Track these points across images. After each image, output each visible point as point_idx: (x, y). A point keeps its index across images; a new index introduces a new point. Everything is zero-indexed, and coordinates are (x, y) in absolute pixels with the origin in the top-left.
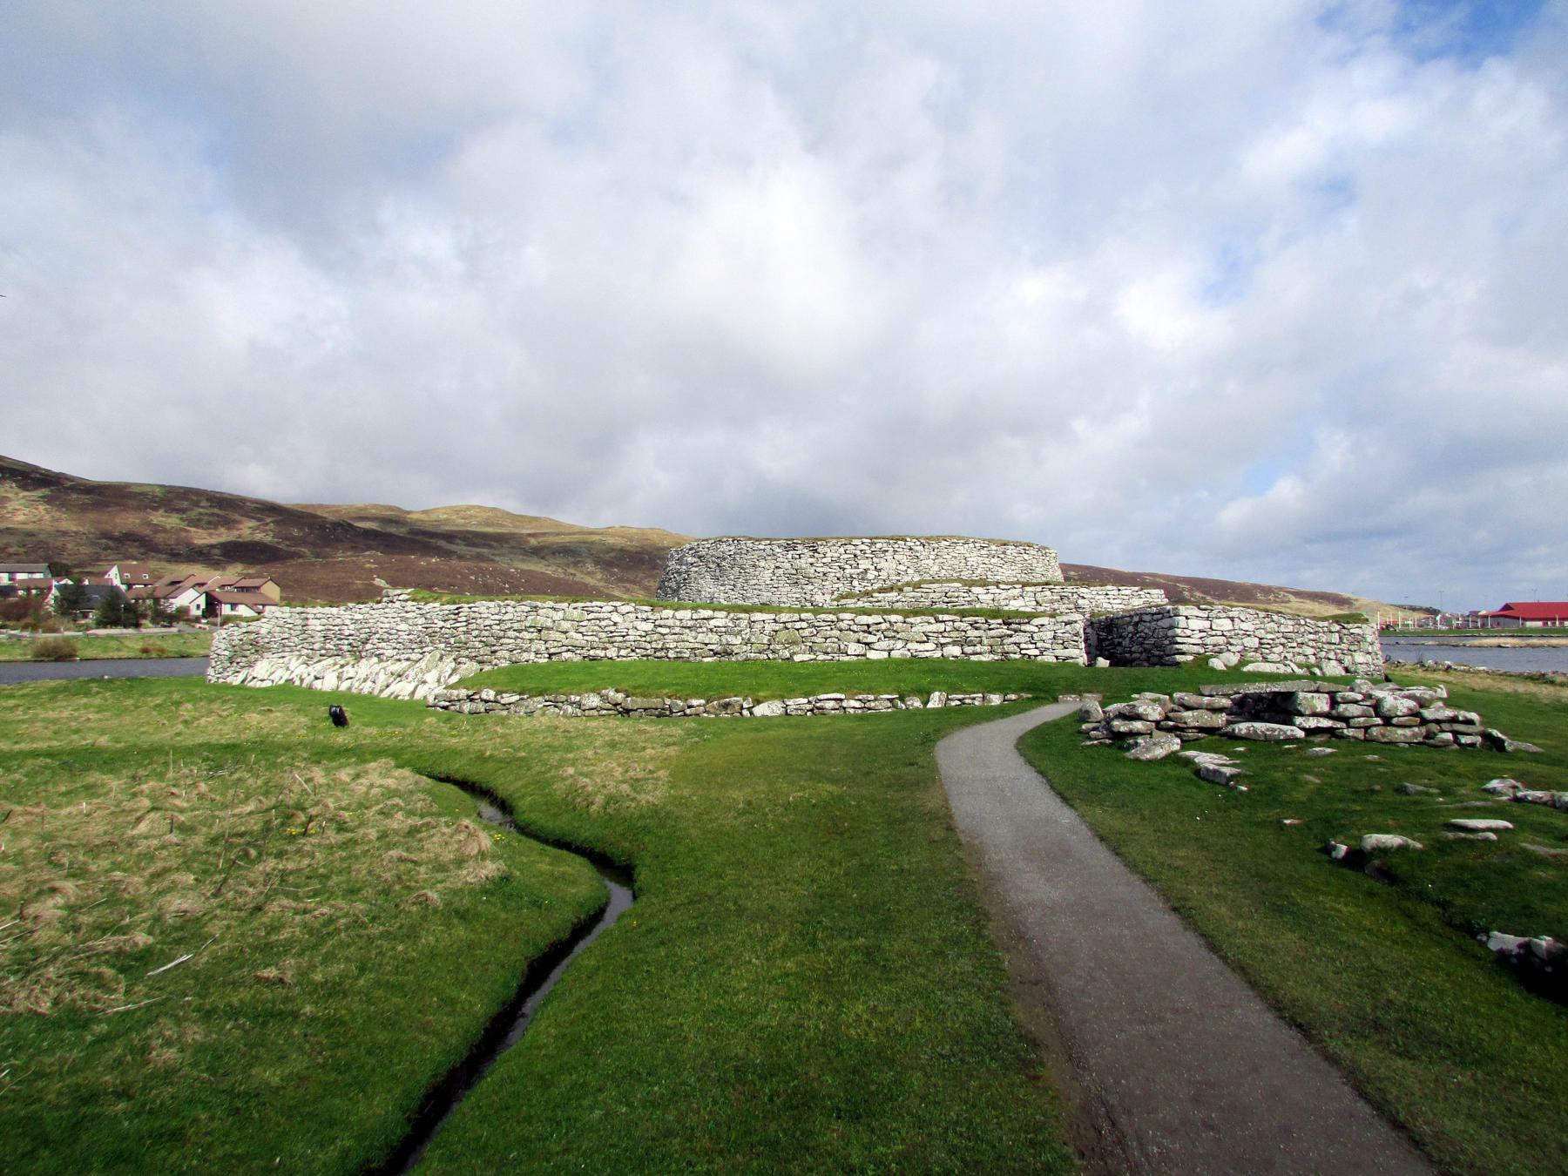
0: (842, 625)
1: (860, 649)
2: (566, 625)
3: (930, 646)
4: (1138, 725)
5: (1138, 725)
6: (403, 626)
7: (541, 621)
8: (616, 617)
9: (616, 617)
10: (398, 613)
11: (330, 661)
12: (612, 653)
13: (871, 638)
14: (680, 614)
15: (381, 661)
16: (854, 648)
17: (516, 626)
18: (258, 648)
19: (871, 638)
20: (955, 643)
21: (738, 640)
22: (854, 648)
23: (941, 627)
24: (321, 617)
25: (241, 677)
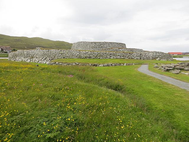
0: (107, 54)
1: (110, 57)
2: (66, 53)
3: (119, 57)
4: (171, 68)
5: (171, 68)
6: (40, 53)
7: (62, 52)
8: (73, 52)
9: (73, 52)
10: (38, 51)
11: (29, 58)
12: (73, 57)
13: (111, 56)
14: (83, 52)
15: (36, 58)
16: (109, 57)
17: (58, 53)
18: (16, 56)
19: (111, 56)
20: (122, 56)
21: (92, 56)
22: (109, 57)
23: (121, 54)
24: (25, 52)
25: (14, 60)
